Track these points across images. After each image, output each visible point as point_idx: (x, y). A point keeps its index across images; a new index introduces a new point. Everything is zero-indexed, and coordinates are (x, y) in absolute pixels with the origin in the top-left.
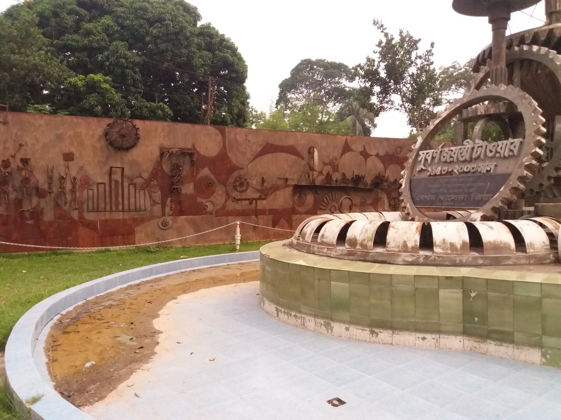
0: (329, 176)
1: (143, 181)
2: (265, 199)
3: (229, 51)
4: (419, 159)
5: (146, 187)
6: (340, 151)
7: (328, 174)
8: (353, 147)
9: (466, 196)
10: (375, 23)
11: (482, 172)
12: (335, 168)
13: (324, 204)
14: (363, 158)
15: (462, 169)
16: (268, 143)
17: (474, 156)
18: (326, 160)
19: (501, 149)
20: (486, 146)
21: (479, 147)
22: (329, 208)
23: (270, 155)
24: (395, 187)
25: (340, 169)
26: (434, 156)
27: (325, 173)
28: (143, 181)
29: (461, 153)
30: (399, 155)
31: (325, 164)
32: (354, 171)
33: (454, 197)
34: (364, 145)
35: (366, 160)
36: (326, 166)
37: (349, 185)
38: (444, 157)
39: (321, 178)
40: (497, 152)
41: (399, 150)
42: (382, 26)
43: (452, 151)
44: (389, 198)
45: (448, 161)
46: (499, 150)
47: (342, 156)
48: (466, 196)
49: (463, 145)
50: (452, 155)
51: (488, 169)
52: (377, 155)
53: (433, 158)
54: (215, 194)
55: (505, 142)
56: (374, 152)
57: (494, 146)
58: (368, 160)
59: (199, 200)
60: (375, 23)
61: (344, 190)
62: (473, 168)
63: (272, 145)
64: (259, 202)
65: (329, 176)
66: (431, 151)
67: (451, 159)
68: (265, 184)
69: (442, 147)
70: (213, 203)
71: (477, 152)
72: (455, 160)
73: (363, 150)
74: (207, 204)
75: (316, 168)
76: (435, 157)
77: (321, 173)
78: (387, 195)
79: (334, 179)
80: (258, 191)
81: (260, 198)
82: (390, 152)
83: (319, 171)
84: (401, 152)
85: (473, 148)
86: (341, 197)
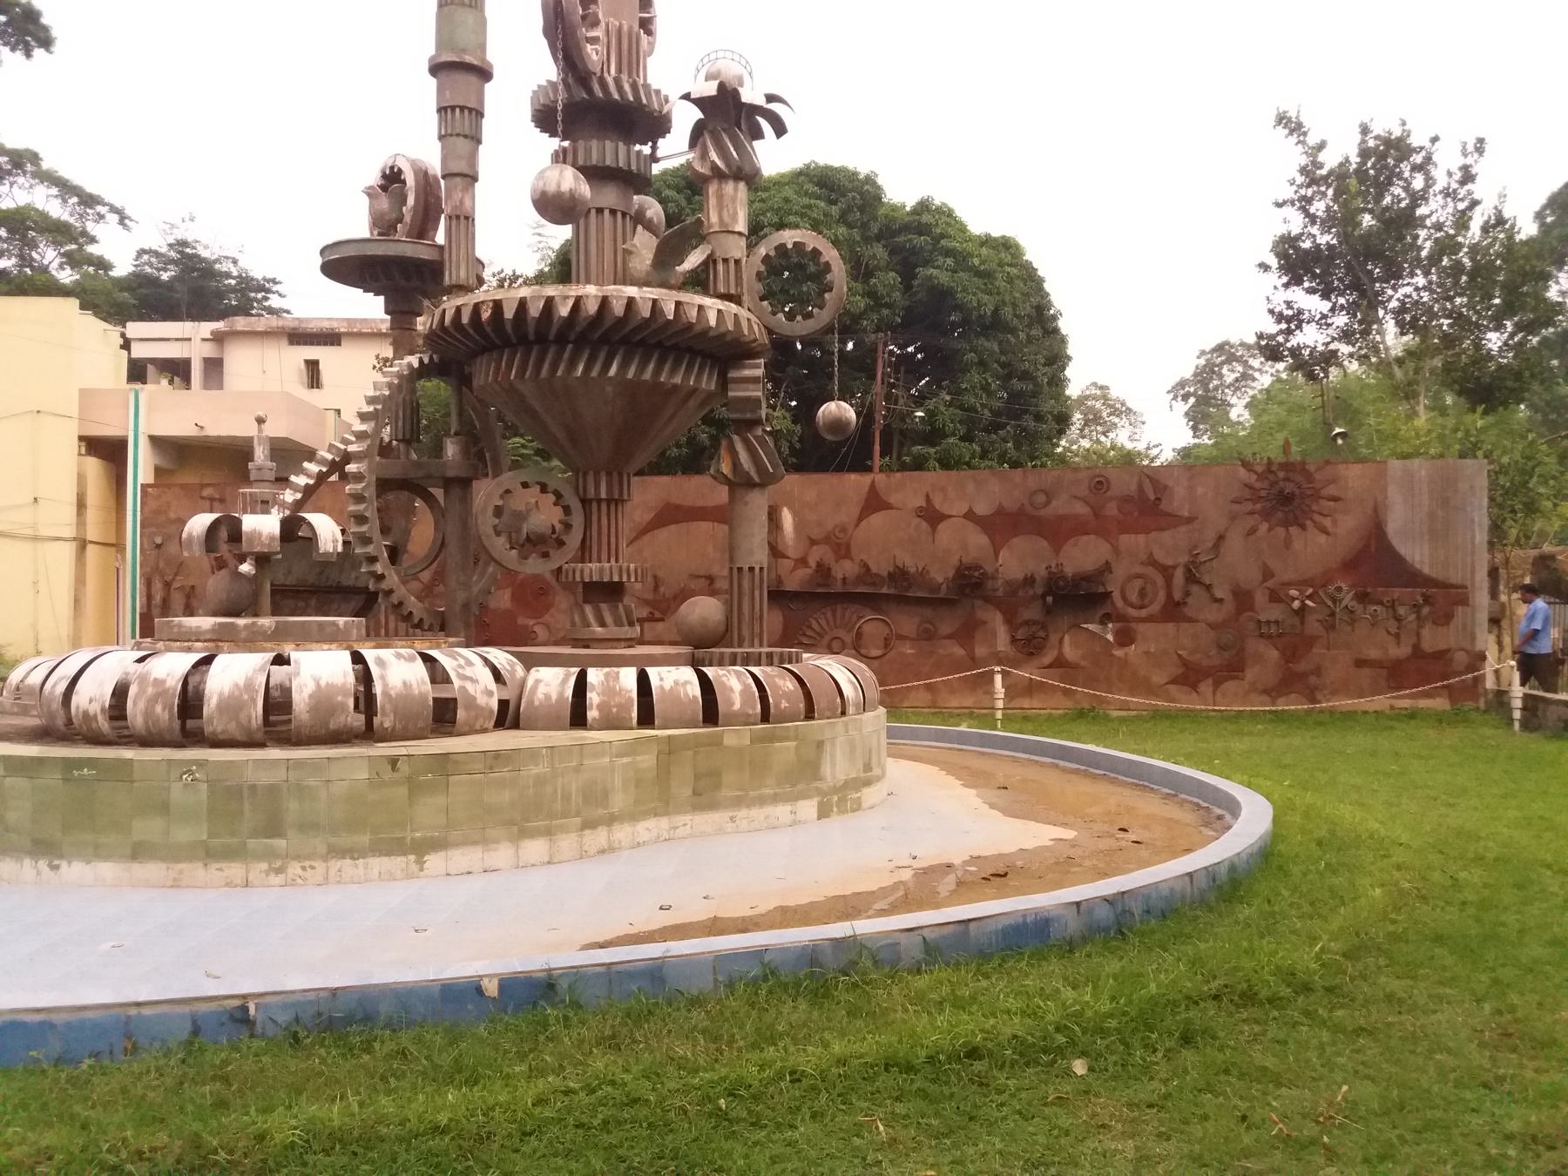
0: (823, 571)
1: (421, 586)
2: (662, 620)
3: (949, 261)
5: (427, 596)
6: (856, 511)
7: (819, 565)
8: (893, 499)
10: (1282, 119)
12: (843, 550)
13: (809, 633)
14: (924, 525)
16: (668, 504)
18: (816, 533)
22: (826, 641)
23: (673, 527)
24: (1031, 592)
25: (854, 552)
27: (812, 562)
28: (421, 586)
30: (1042, 512)
31: (813, 542)
34: (928, 496)
36: (815, 547)
37: (885, 590)
39: (803, 573)
41: (1041, 498)
42: (1300, 125)
44: (1010, 621)
47: (860, 519)
52: (970, 516)
54: (553, 610)
56: (960, 508)
58: (942, 527)
59: (521, 621)
60: (1282, 119)
61: (871, 601)
63: (678, 507)
64: (646, 625)
65: (823, 571)
68: (662, 589)
70: (548, 626)
73: (922, 502)
74: (536, 629)
75: (791, 553)
77: (802, 562)
78: (1004, 613)
79: (840, 576)
80: (647, 602)
81: (651, 619)
82: (1010, 505)
83: (799, 556)
84: (1048, 502)
86: (860, 618)
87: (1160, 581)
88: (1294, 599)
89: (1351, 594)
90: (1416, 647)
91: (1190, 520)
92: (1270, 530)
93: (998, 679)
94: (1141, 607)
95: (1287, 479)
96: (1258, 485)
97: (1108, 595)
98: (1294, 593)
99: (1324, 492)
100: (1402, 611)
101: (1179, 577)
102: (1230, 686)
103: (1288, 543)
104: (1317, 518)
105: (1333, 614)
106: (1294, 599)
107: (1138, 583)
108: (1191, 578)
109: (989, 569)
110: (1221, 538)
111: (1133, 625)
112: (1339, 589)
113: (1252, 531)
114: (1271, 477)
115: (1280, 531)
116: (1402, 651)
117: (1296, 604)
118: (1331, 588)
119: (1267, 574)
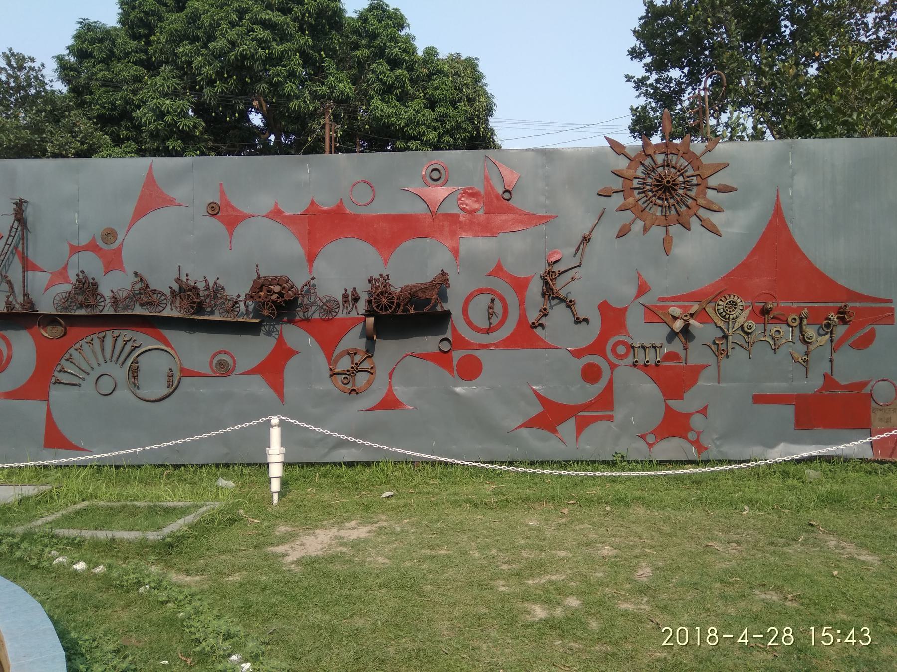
6: (130, 209)
8: (179, 192)
12: (113, 261)
27: (72, 276)
32: (179, 266)
35: (231, 234)
52: (276, 214)
56: (263, 202)
58: (240, 229)
77: (61, 274)
87: (512, 298)
88: (675, 318)
89: (747, 312)
90: (828, 379)
91: (545, 219)
92: (646, 230)
93: (275, 434)
94: (489, 331)
95: (667, 164)
96: (630, 173)
97: (447, 314)
98: (676, 311)
99: (713, 181)
100: (811, 331)
101: (535, 288)
102: (599, 427)
103: (667, 245)
104: (702, 212)
105: (725, 337)
106: (675, 318)
107: (485, 299)
108: (549, 292)
109: (299, 281)
110: (586, 240)
111: (479, 354)
112: (733, 304)
113: (623, 233)
114: (648, 162)
115: (657, 232)
116: (813, 384)
117: (678, 325)
118: (722, 305)
119: (643, 289)
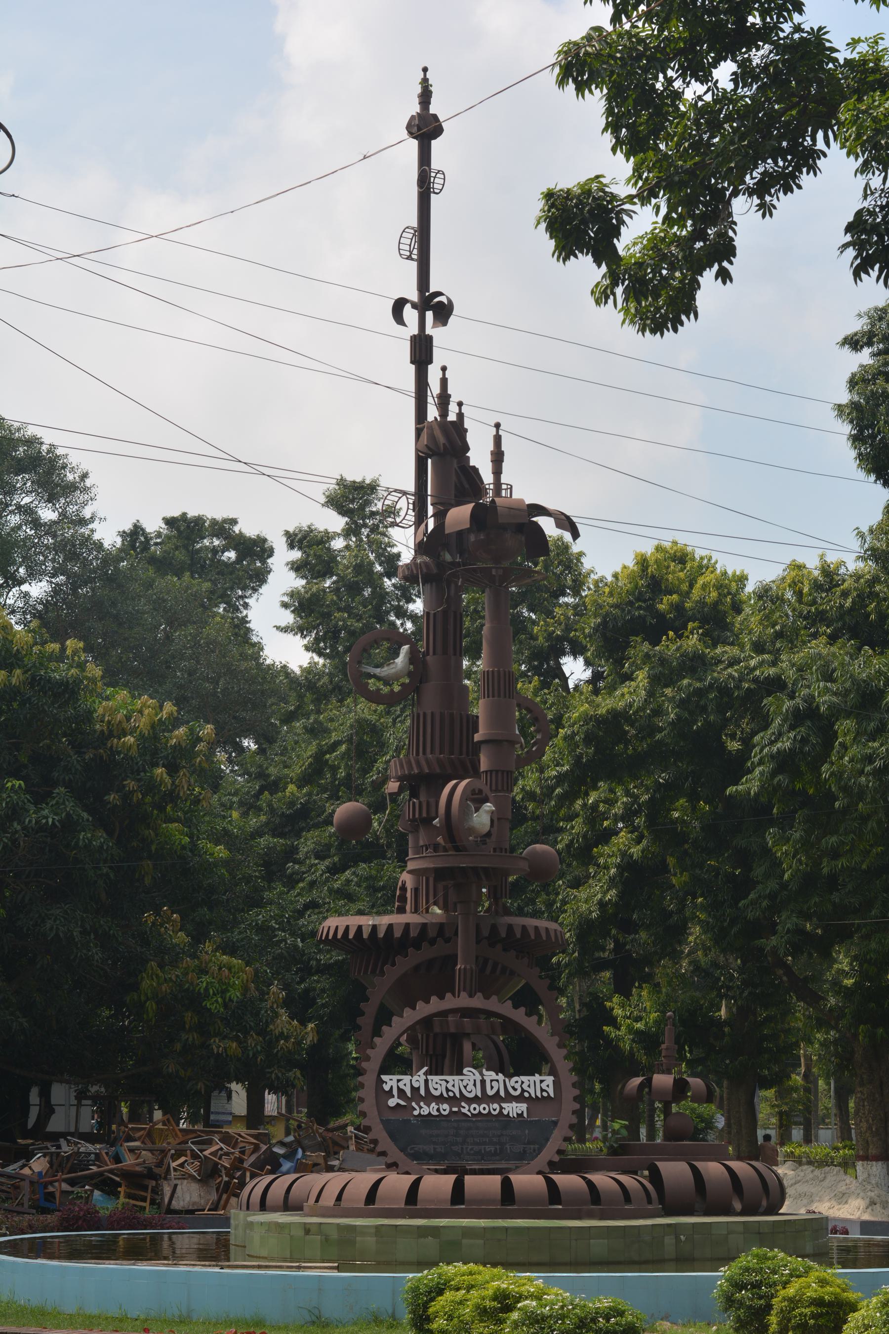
4: (386, 1088)
9: (498, 1147)
11: (511, 1115)
15: (475, 1109)
17: (490, 1093)
19: (529, 1086)
20: (504, 1081)
21: (492, 1081)
26: (416, 1085)
29: (465, 1087)
33: (476, 1148)
38: (436, 1089)
40: (523, 1091)
43: (447, 1082)
45: (445, 1095)
46: (525, 1086)
48: (498, 1147)
49: (462, 1074)
50: (450, 1088)
51: (520, 1112)
53: (415, 1090)
55: (531, 1078)
57: (517, 1082)
62: (495, 1110)
66: (406, 1079)
67: (451, 1094)
69: (426, 1074)
71: (492, 1088)
72: (458, 1095)
76: (419, 1088)
85: (483, 1082)
